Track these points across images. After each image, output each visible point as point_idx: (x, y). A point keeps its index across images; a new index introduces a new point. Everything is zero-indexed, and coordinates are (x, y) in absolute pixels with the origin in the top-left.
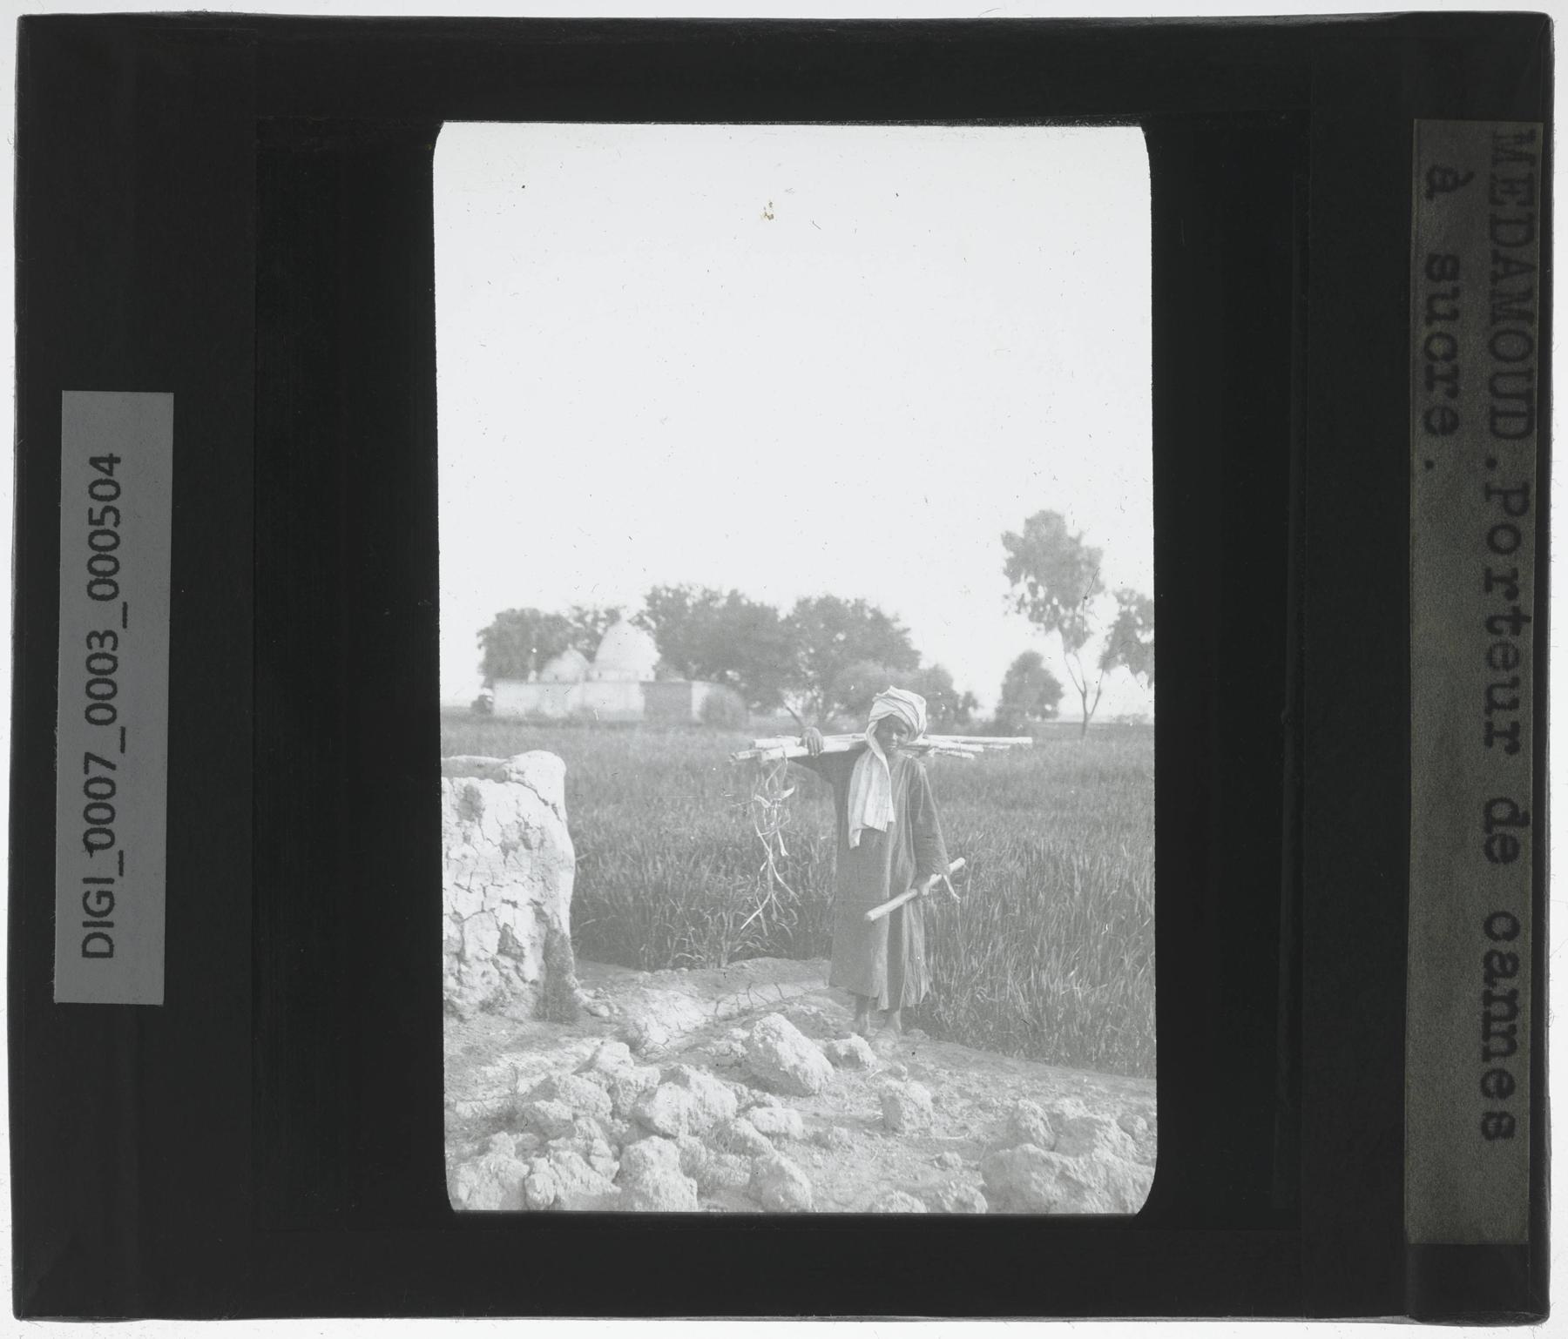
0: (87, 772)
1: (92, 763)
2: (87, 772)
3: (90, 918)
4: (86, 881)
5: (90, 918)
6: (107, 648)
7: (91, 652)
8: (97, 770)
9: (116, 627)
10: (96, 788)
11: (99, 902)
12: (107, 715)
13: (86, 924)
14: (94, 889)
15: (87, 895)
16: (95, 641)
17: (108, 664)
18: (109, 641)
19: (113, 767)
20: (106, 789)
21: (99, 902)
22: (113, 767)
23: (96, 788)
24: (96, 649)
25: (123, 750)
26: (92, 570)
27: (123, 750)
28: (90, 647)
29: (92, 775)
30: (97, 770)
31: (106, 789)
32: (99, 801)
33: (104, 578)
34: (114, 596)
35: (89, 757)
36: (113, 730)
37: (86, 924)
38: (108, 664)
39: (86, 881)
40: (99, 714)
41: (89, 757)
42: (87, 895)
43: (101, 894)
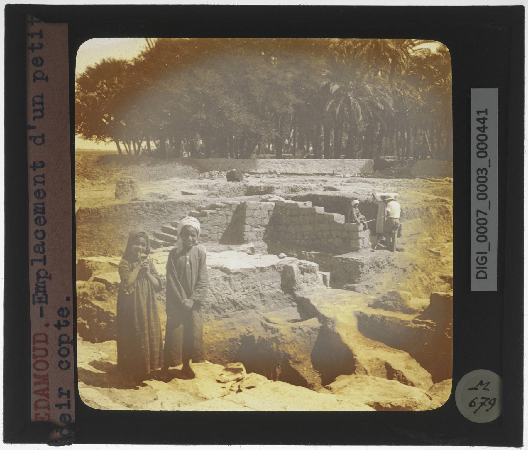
0: (477, 216)
1: (479, 213)
2: (477, 216)
3: (480, 266)
4: (478, 253)
5: (480, 266)
6: (484, 174)
7: (478, 176)
8: (481, 215)
9: (486, 166)
10: (480, 222)
11: (482, 260)
12: (484, 197)
13: (478, 268)
14: (480, 255)
15: (478, 257)
16: (480, 172)
17: (484, 180)
18: (484, 172)
19: (486, 214)
20: (484, 222)
21: (482, 260)
22: (486, 214)
23: (480, 222)
24: (480, 175)
25: (489, 208)
26: (478, 148)
27: (489, 208)
28: (478, 174)
29: (478, 218)
30: (481, 215)
31: (484, 222)
32: (482, 226)
33: (482, 150)
34: (486, 156)
35: (478, 211)
36: (487, 201)
37: (478, 268)
38: (484, 180)
39: (478, 253)
40: (481, 197)
41: (478, 211)
42: (478, 257)
43: (482, 258)
